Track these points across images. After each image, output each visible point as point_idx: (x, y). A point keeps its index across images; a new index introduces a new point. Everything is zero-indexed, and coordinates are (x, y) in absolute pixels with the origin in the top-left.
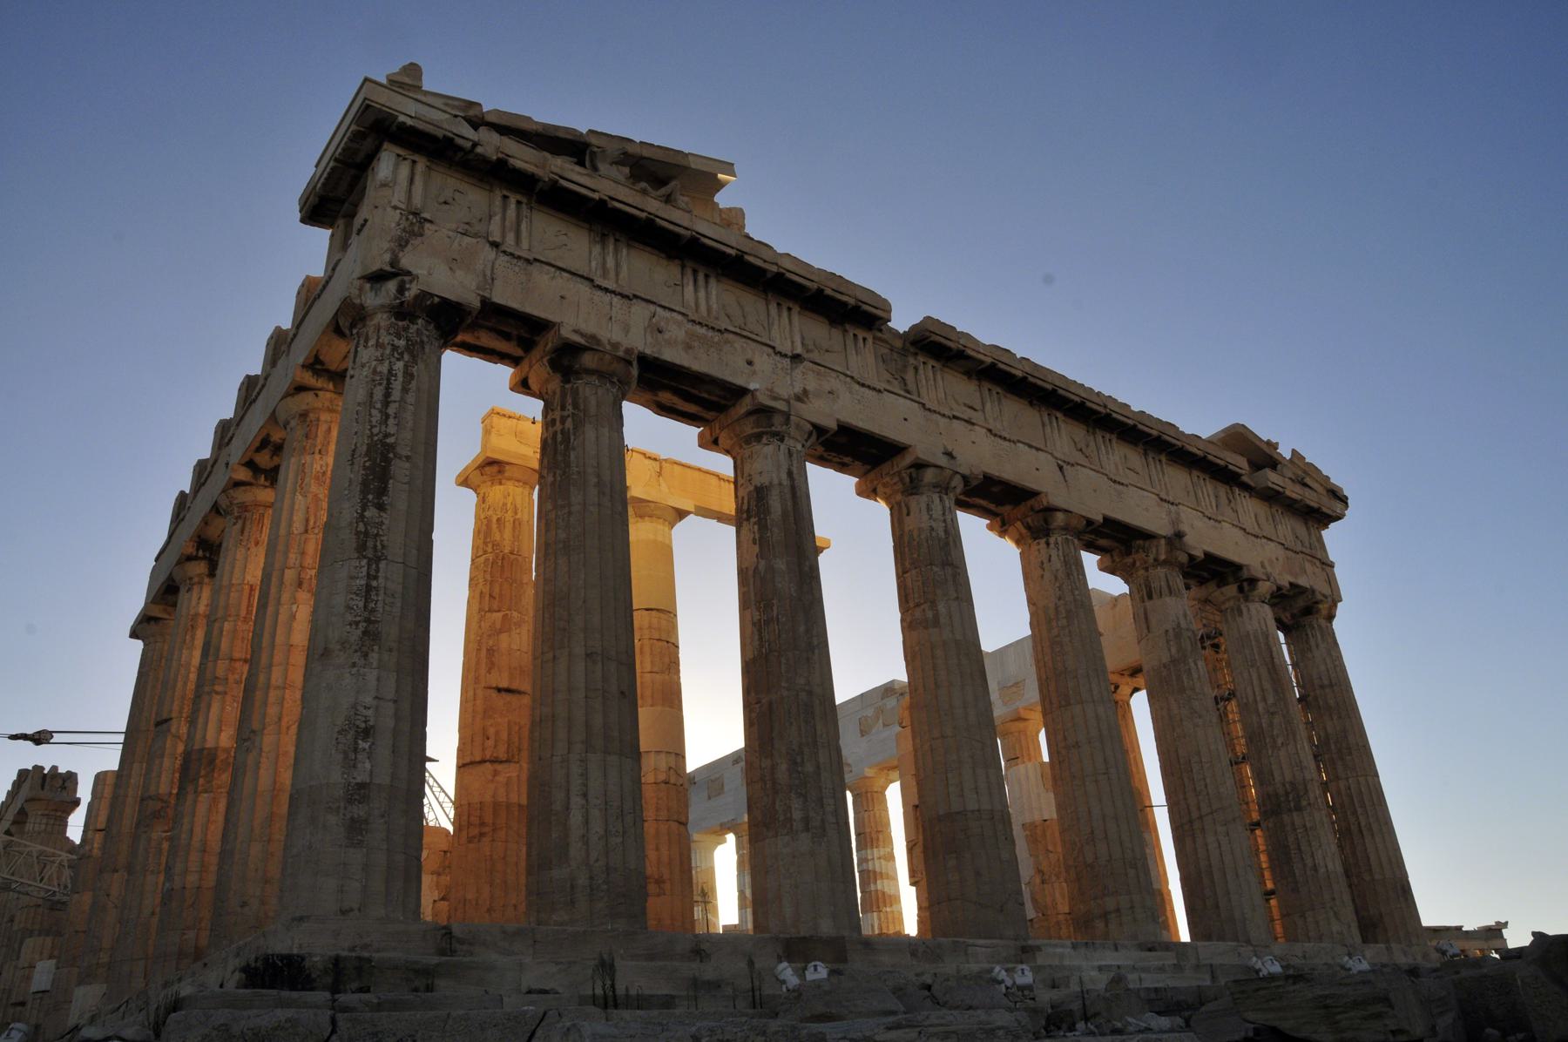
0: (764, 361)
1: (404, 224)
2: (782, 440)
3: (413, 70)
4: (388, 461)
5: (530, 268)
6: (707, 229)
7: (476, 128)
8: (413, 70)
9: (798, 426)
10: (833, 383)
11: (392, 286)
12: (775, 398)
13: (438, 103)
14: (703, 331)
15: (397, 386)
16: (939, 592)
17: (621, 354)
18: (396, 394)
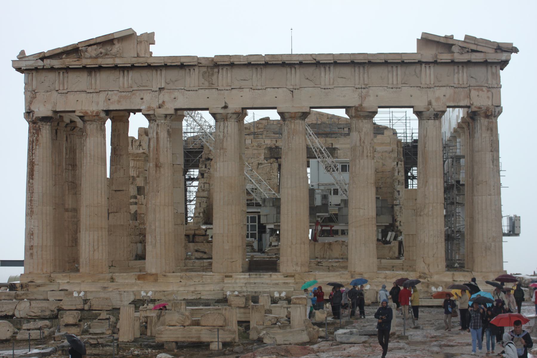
0: (147, 96)
1: (32, 95)
2: (156, 121)
3: (23, 52)
4: (33, 166)
5: (67, 95)
6: (119, 62)
7: (43, 61)
8: (23, 52)
9: (159, 117)
10: (176, 94)
11: (31, 114)
12: (149, 111)
13: (31, 58)
14: (125, 94)
15: (34, 144)
16: (218, 159)
17: (94, 114)
18: (34, 147)
